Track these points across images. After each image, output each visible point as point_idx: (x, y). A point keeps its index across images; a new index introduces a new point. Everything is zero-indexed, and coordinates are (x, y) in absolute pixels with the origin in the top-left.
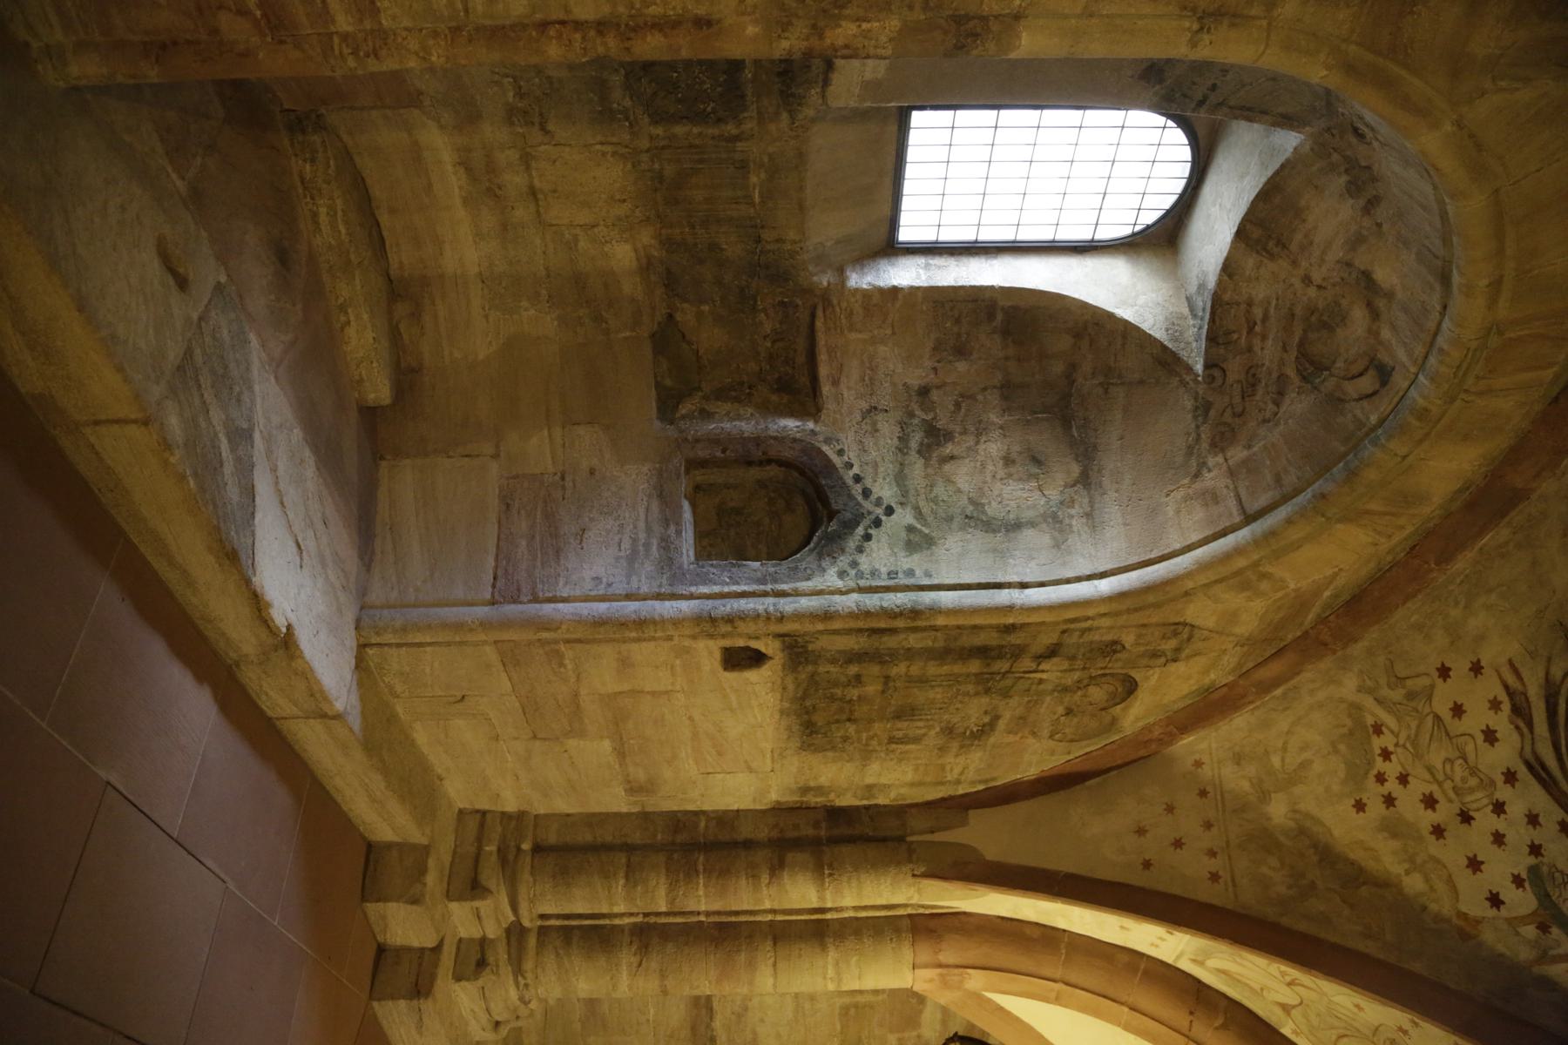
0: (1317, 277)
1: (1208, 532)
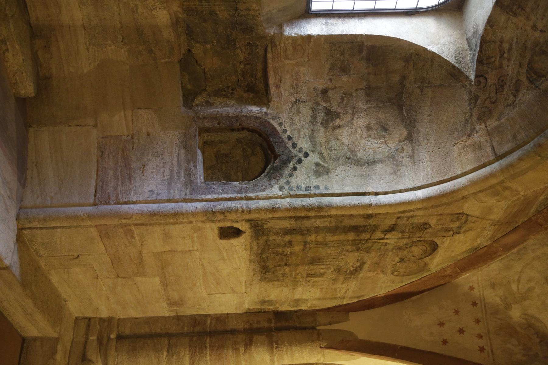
0: (540, 25)
1: (475, 165)
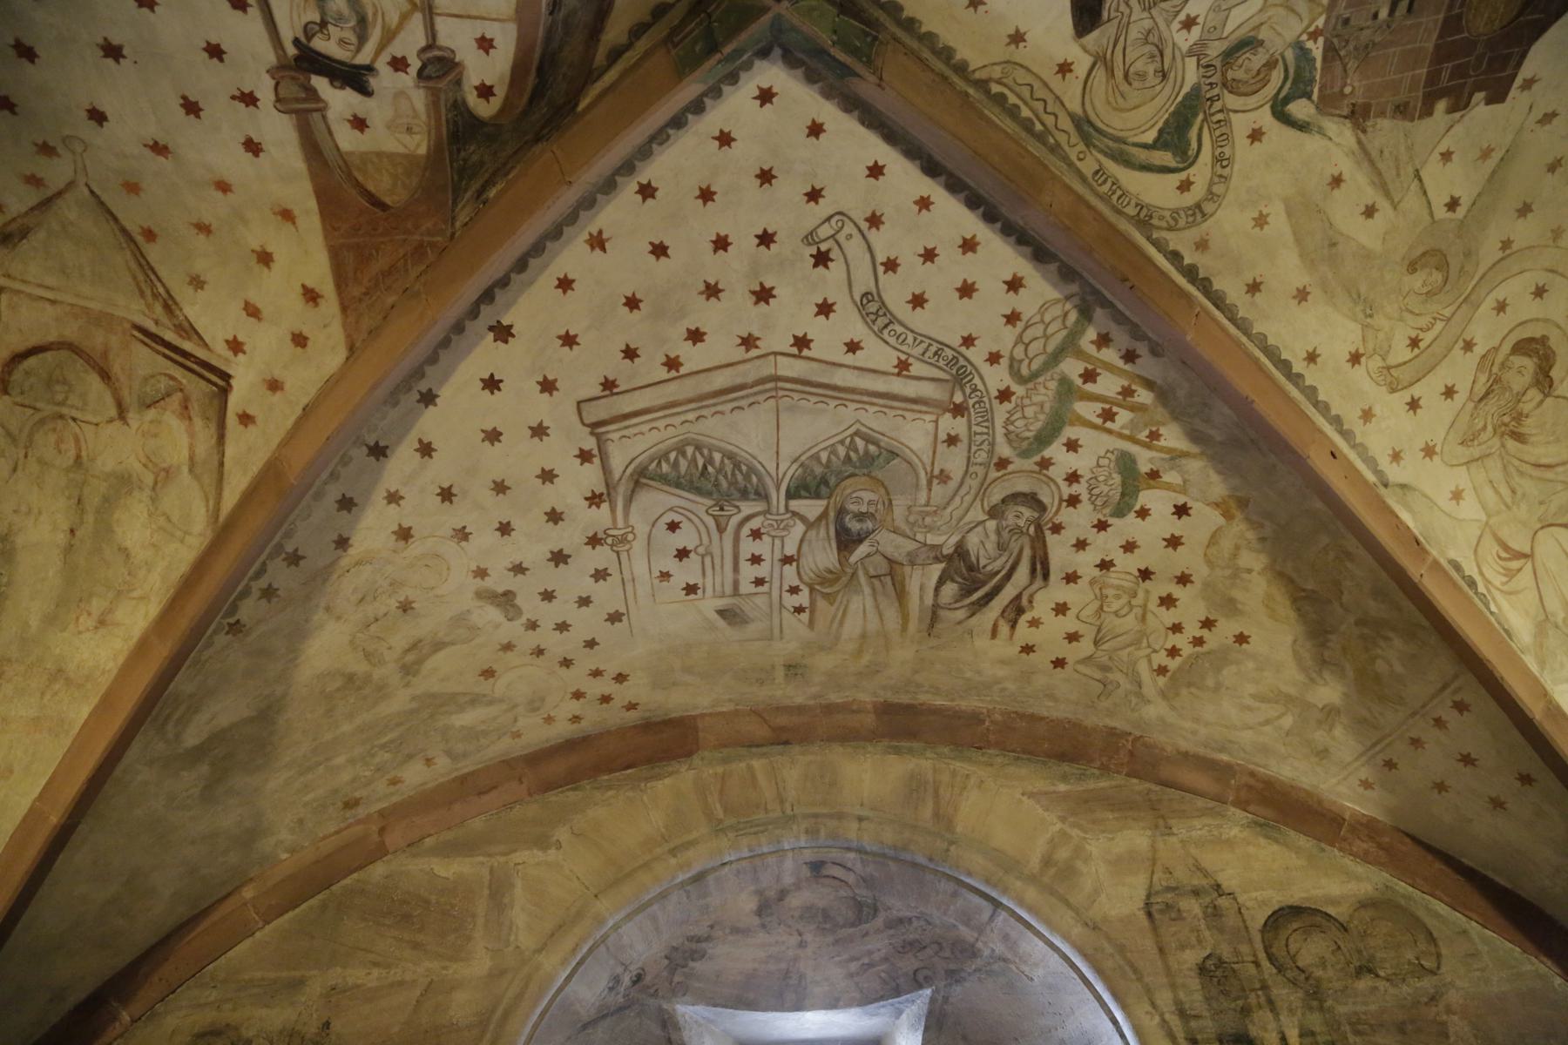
0: (794, 940)
1: (1029, 934)
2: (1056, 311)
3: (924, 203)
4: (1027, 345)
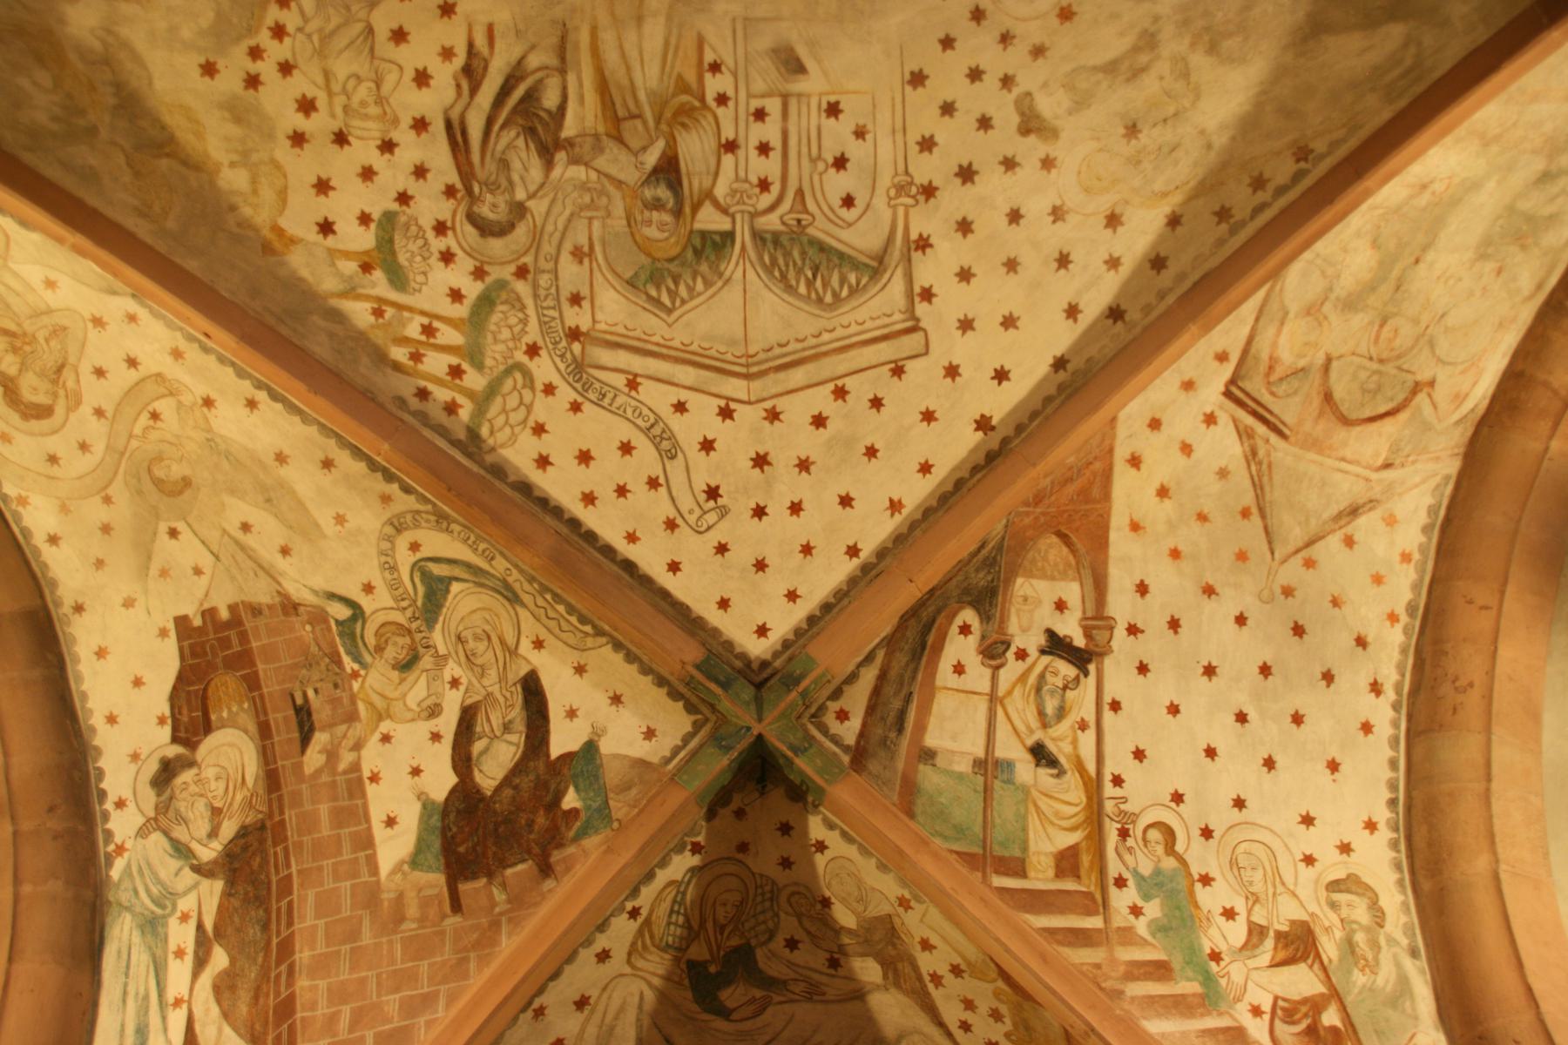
2: (502, 437)
3: (632, 538)
4: (521, 403)
